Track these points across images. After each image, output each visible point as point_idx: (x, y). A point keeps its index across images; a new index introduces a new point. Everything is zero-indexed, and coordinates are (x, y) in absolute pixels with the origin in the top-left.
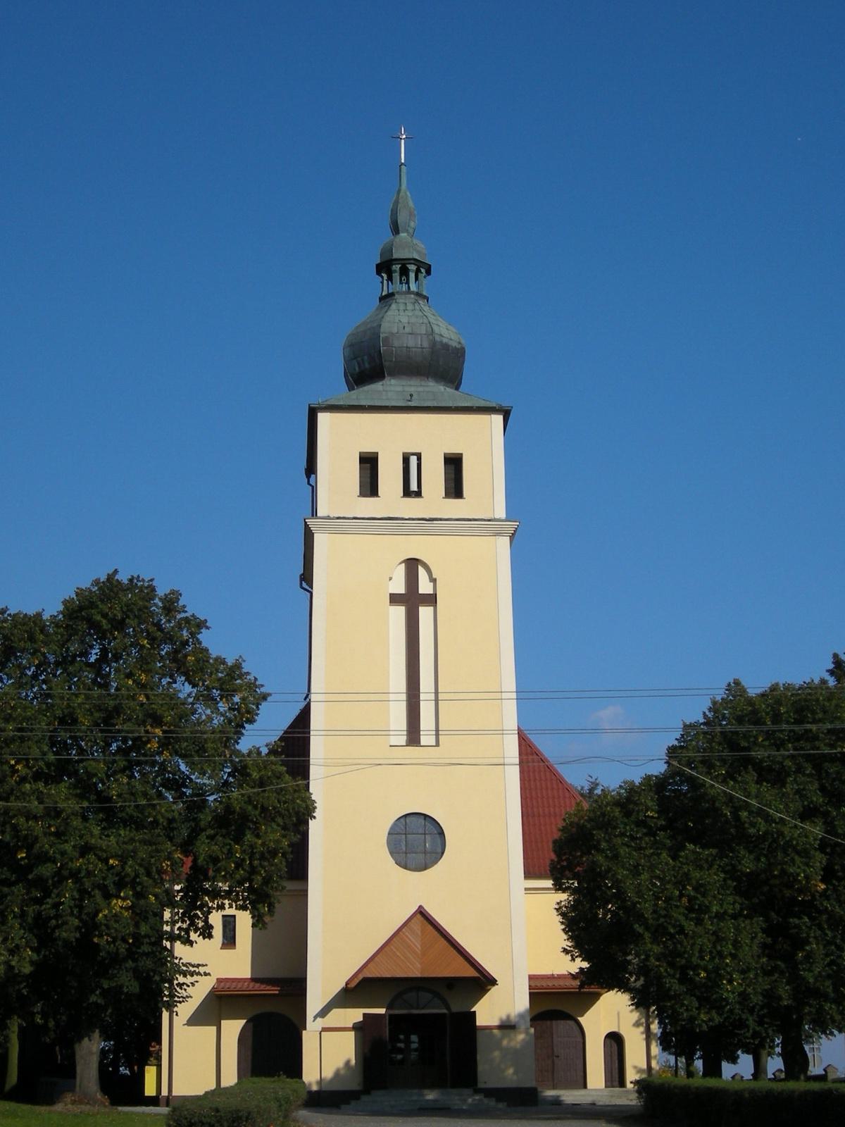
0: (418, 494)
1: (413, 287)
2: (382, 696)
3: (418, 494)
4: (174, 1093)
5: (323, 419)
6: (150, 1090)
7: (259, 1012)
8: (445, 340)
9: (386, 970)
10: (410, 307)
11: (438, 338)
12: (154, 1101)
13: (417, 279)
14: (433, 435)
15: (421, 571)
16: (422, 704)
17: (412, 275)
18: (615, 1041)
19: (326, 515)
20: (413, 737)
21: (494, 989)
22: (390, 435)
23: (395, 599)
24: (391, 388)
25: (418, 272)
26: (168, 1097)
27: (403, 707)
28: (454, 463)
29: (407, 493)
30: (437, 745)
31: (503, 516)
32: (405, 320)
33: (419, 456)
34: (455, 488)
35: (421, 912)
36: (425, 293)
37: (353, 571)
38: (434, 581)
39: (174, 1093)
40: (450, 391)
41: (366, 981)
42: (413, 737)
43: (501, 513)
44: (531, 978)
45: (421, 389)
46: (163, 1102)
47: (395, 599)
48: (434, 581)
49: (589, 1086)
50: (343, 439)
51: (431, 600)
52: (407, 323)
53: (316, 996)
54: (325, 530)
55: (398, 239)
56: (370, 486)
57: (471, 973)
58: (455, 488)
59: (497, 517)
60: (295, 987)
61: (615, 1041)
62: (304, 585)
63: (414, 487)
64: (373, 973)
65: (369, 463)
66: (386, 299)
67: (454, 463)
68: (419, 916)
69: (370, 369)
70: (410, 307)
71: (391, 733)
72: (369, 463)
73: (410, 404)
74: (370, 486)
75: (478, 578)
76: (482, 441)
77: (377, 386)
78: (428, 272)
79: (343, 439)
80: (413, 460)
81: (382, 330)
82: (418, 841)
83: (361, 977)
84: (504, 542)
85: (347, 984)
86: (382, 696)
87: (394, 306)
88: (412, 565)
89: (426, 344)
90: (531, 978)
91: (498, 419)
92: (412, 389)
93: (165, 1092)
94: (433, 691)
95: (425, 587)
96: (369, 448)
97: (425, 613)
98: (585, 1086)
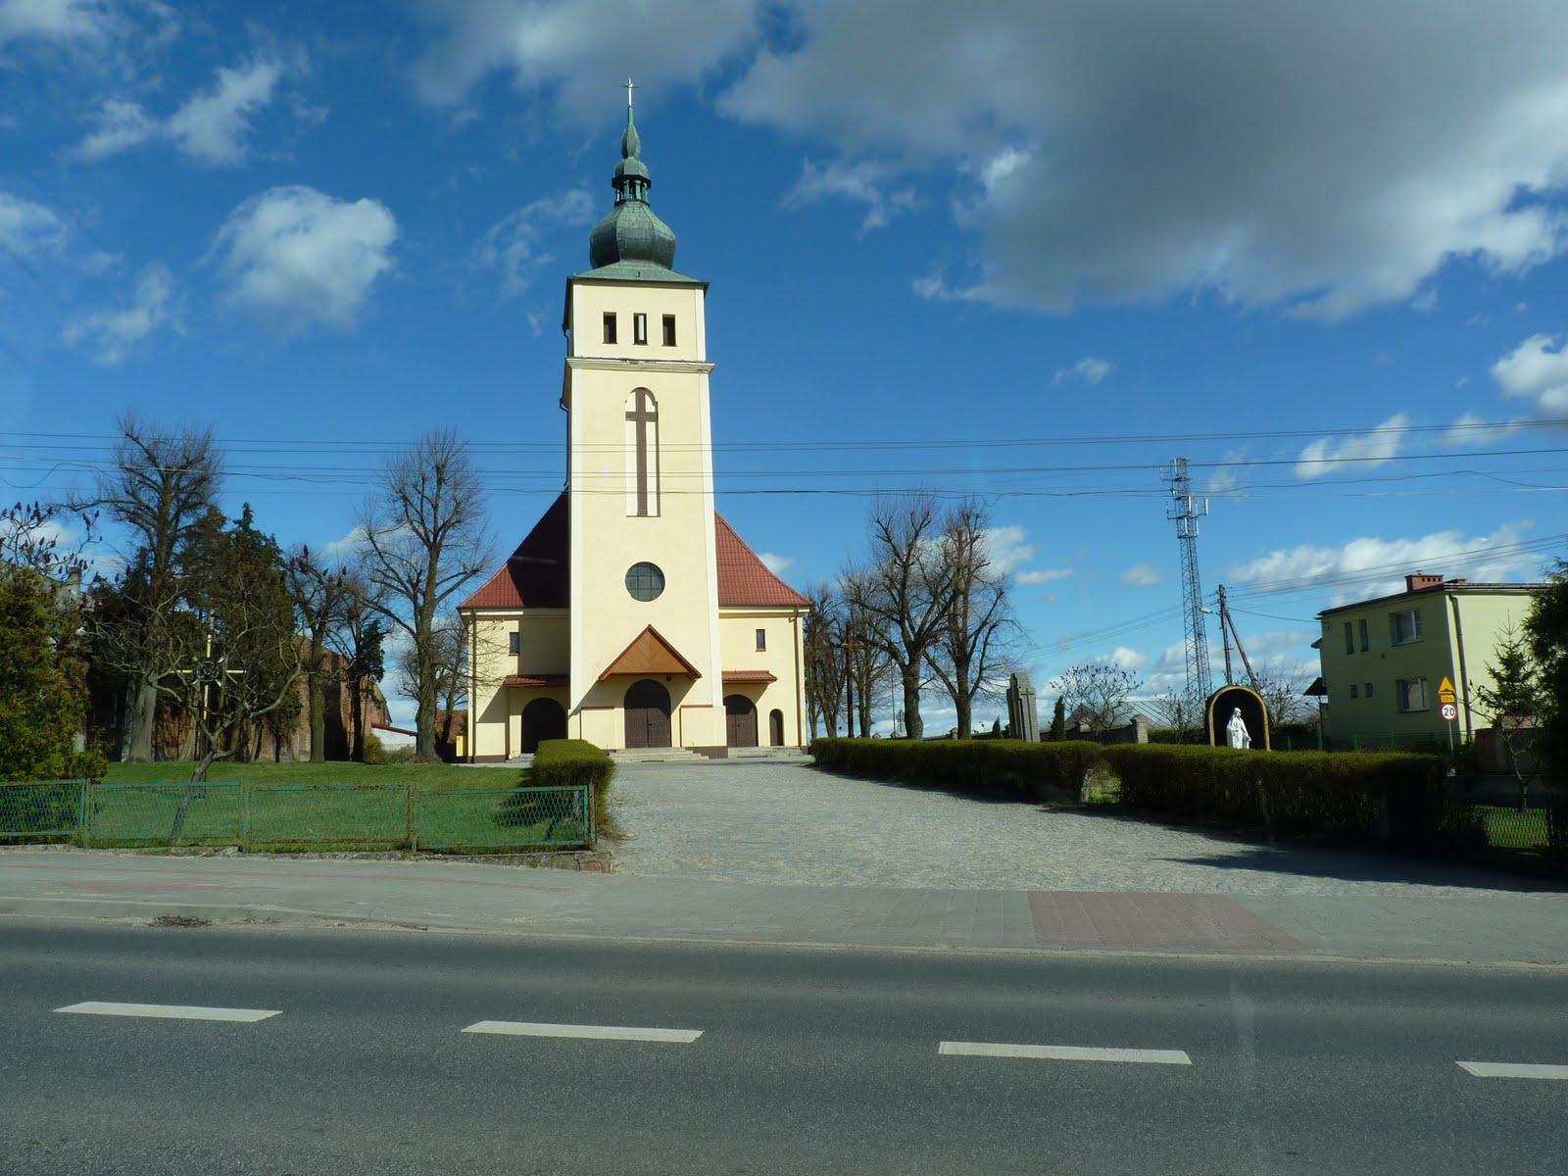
0: (644, 342)
1: (639, 196)
2: (622, 475)
3: (644, 342)
4: (477, 754)
5: (577, 289)
6: (459, 753)
7: (535, 697)
8: (662, 235)
9: (627, 668)
10: (637, 210)
11: (657, 233)
12: (464, 759)
13: (641, 191)
14: (656, 302)
15: (648, 399)
16: (648, 454)
17: (638, 188)
18: (777, 716)
19: (580, 355)
20: (642, 511)
21: (698, 681)
22: (625, 301)
23: (629, 416)
24: (624, 268)
25: (642, 186)
26: (473, 757)
27: (634, 456)
28: (669, 322)
29: (637, 341)
30: (659, 515)
31: (704, 360)
32: (634, 219)
33: (645, 316)
34: (670, 339)
35: (650, 630)
36: (647, 201)
37: (598, 400)
38: (655, 404)
39: (477, 754)
40: (666, 270)
41: (611, 675)
42: (642, 511)
43: (702, 357)
44: (724, 673)
45: (646, 269)
46: (469, 760)
47: (629, 416)
48: (655, 404)
49: (760, 744)
50: (590, 303)
51: (655, 417)
52: (637, 219)
53: (581, 684)
54: (578, 366)
55: (627, 160)
56: (611, 337)
57: (684, 670)
58: (670, 339)
59: (699, 360)
60: (561, 679)
61: (777, 716)
62: (563, 406)
63: (642, 338)
64: (617, 670)
65: (610, 321)
66: (621, 203)
67: (669, 322)
68: (648, 634)
69: (607, 250)
70: (637, 210)
71: (627, 475)
72: (610, 321)
73: (638, 279)
74: (611, 337)
75: (688, 406)
76: (690, 307)
77: (615, 266)
78: (649, 186)
79: (590, 303)
80: (641, 318)
81: (618, 225)
82: (646, 580)
83: (609, 673)
84: (705, 377)
85: (600, 678)
86: (622, 475)
87: (625, 209)
88: (641, 392)
89: (649, 237)
90: (724, 673)
91: (700, 293)
92: (639, 269)
93: (470, 754)
94: (655, 490)
95: (649, 408)
96: (610, 310)
97: (650, 426)
98: (757, 745)
